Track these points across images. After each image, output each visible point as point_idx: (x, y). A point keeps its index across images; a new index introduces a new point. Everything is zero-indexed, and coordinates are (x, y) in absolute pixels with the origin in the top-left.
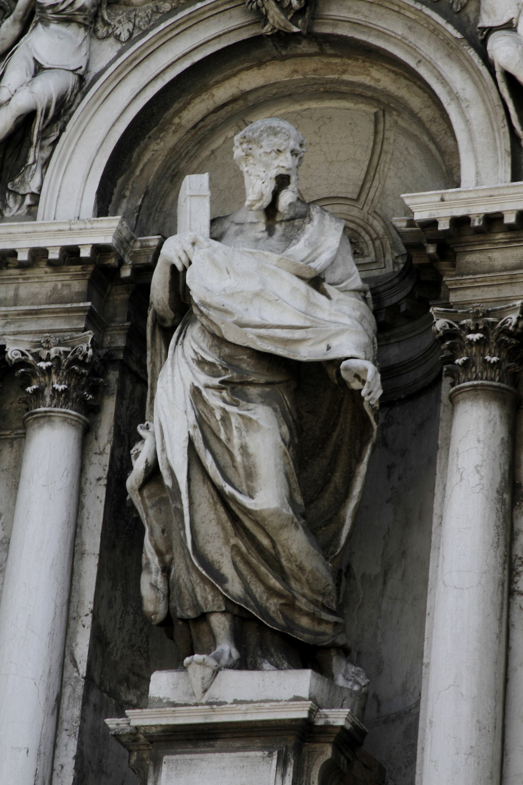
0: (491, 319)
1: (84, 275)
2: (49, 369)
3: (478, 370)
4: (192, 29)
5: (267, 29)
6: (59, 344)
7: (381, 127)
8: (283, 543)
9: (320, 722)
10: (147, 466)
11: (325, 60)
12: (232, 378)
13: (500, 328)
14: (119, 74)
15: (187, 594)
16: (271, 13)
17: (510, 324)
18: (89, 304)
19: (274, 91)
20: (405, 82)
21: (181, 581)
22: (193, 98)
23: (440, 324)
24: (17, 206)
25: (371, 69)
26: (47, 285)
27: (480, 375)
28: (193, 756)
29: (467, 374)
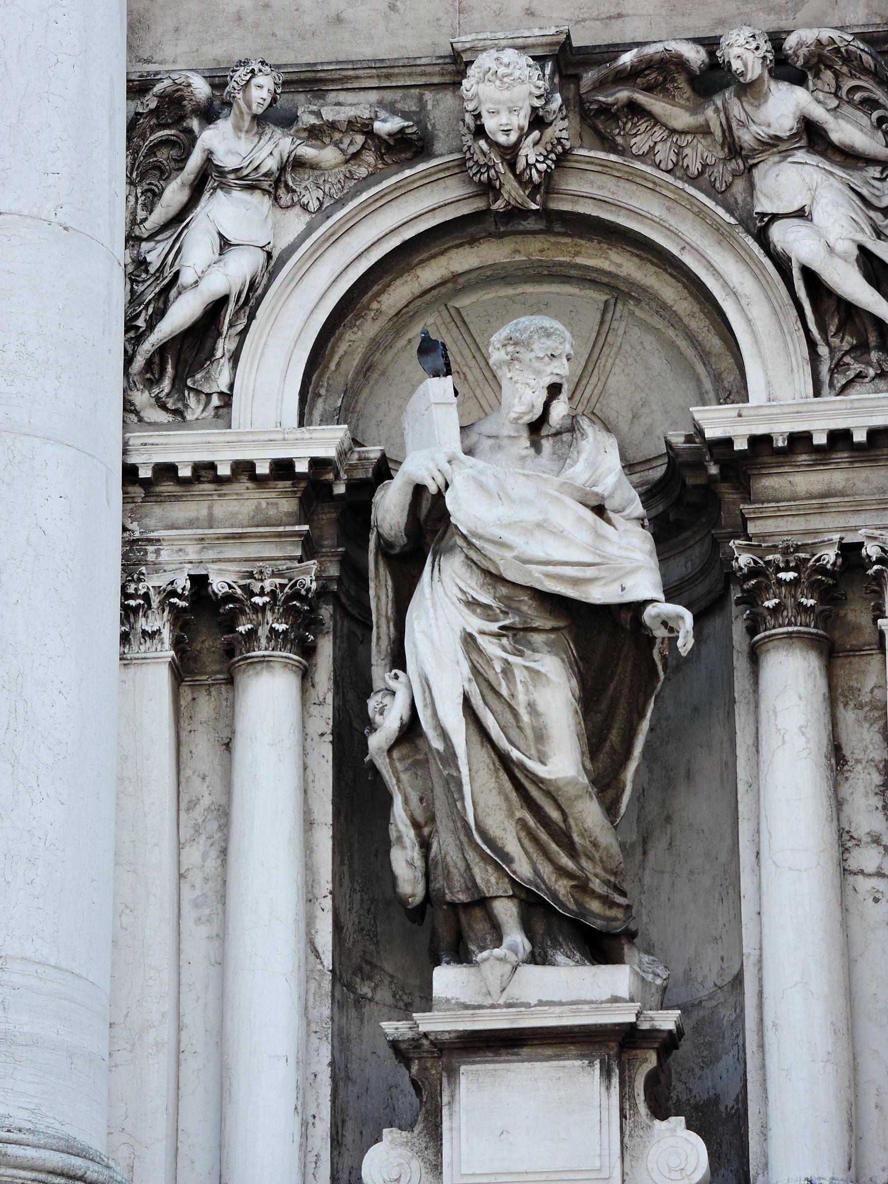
0: (802, 555)
1: (295, 492)
2: (265, 604)
3: (790, 614)
4: (399, 200)
5: (499, 205)
6: (274, 575)
7: (609, 316)
8: (576, 815)
9: (645, 1026)
10: (402, 723)
11: (553, 239)
12: (514, 623)
13: (813, 566)
14: (315, 252)
15: (458, 874)
16: (507, 187)
17: (828, 562)
18: (306, 527)
19: (489, 274)
20: (654, 269)
21: (448, 859)
22: (395, 279)
23: (744, 560)
24: (201, 408)
25: (609, 251)
26: (249, 502)
27: (793, 619)
28: (497, 1066)
29: (776, 619)
